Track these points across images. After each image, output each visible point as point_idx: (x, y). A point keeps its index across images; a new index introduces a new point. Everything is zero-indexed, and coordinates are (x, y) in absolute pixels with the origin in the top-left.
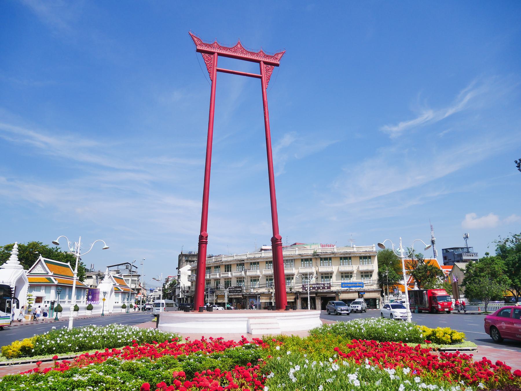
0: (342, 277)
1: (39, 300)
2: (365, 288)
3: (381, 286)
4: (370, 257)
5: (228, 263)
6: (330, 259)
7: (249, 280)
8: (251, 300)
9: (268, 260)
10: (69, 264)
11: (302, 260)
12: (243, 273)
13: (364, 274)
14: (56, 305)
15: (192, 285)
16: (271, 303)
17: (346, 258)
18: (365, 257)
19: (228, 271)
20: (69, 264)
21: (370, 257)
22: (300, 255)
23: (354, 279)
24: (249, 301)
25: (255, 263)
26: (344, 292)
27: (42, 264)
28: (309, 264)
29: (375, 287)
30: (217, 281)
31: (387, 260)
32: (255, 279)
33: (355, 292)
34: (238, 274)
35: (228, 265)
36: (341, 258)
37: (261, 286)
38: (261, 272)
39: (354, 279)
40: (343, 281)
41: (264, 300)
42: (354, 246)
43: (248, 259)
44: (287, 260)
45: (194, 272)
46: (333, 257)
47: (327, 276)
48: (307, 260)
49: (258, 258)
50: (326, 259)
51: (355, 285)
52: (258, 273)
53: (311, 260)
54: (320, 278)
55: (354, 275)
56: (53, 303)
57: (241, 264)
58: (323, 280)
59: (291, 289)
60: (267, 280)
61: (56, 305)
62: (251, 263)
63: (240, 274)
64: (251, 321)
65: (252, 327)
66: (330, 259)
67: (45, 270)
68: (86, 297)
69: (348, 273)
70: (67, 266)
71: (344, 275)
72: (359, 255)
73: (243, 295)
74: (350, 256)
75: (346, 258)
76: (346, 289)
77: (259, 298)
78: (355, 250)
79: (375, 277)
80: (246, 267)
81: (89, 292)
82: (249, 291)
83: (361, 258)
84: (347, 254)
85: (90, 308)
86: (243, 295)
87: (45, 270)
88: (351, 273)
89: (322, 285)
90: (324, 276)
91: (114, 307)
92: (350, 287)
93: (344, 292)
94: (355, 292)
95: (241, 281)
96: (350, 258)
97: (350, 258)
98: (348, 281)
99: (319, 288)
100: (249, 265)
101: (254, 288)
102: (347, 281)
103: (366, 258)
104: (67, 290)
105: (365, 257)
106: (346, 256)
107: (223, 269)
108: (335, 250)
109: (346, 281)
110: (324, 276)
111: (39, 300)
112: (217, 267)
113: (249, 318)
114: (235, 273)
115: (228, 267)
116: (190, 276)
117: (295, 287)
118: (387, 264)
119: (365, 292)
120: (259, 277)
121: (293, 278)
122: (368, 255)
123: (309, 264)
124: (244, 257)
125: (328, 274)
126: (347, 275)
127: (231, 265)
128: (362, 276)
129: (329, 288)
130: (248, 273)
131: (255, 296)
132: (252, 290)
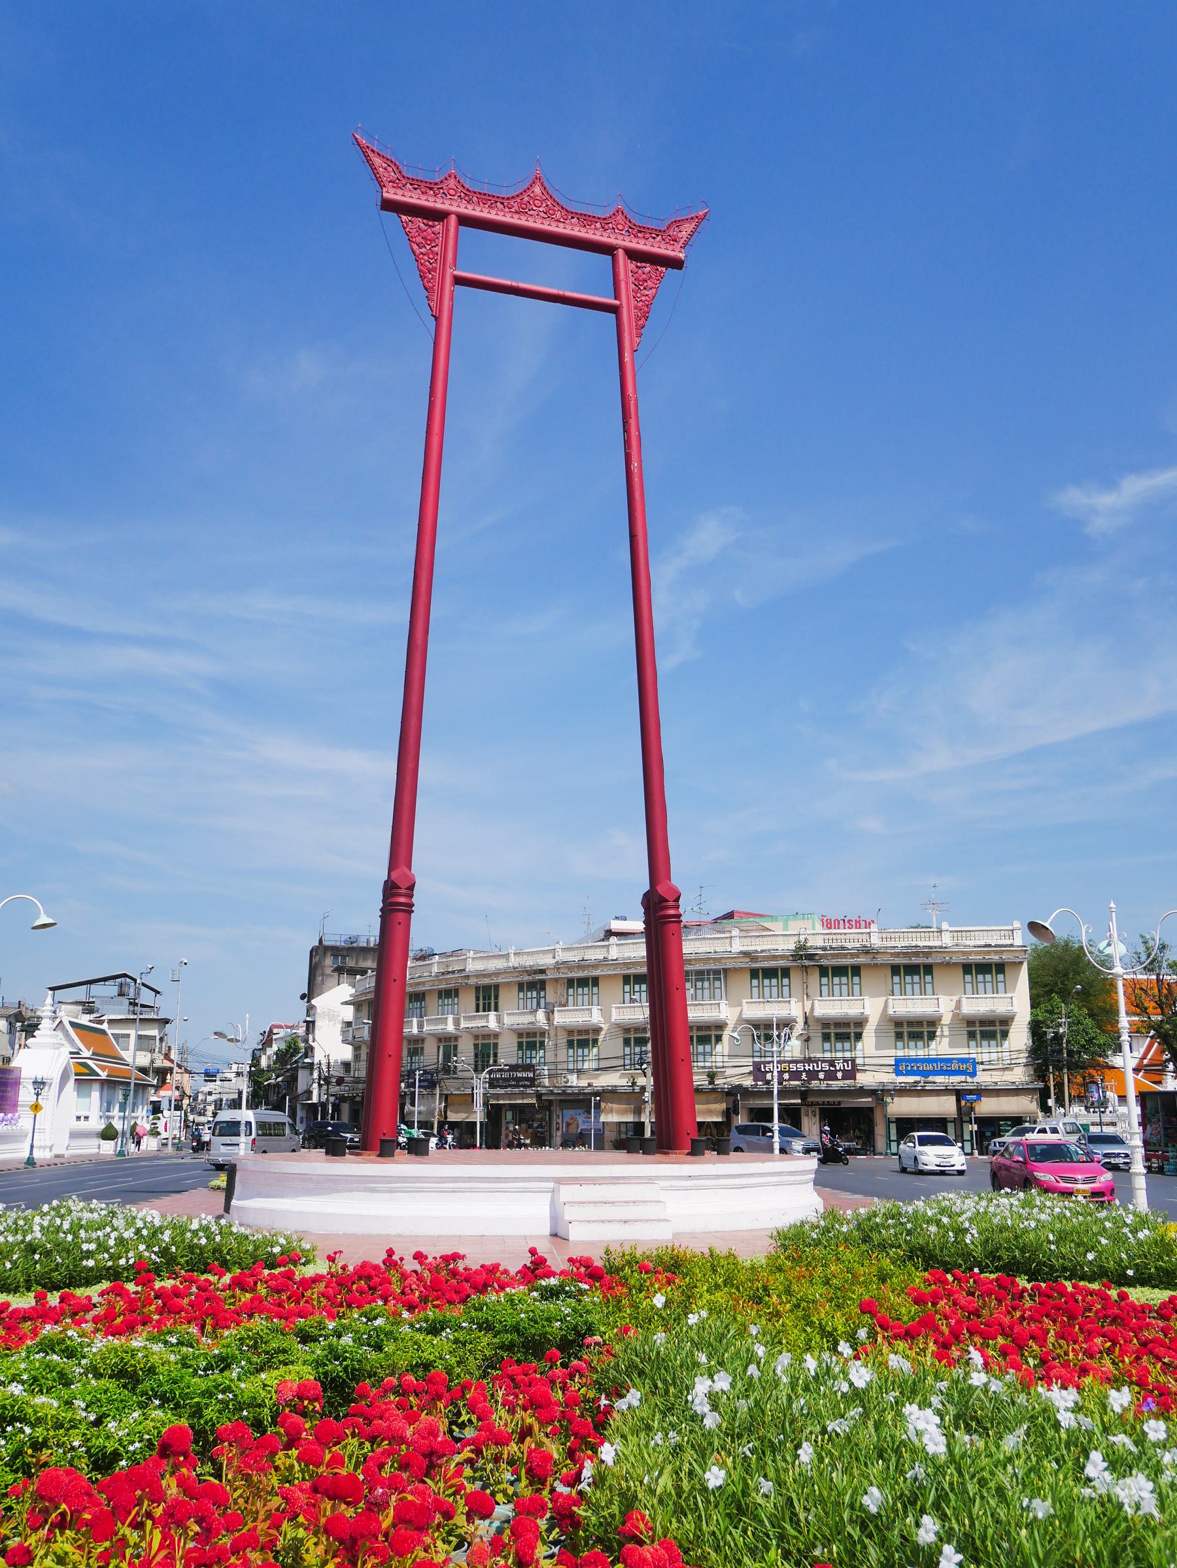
0: (899, 1036)
2: (983, 1078)
3: (1040, 1073)
4: (1000, 968)
5: (487, 981)
6: (856, 970)
7: (563, 1041)
8: (568, 1113)
9: (632, 971)
11: (754, 973)
12: (541, 1015)
13: (978, 1029)
15: (357, 1057)
16: (639, 1126)
17: (914, 968)
18: (984, 968)
19: (487, 1008)
21: (1000, 968)
22: (746, 954)
23: (941, 1047)
24: (563, 1119)
25: (583, 982)
26: (903, 1091)
28: (780, 987)
29: (1019, 1075)
30: (449, 1043)
31: (1064, 977)
32: (583, 1039)
33: (946, 1091)
34: (522, 1020)
35: (487, 988)
36: (895, 970)
37: (603, 1064)
38: (606, 1014)
39: (941, 1047)
40: (900, 1053)
41: (614, 1116)
42: (945, 926)
43: (558, 967)
45: (365, 1010)
46: (868, 966)
47: (846, 1031)
48: (770, 973)
49: (597, 965)
50: (840, 971)
51: (945, 1066)
53: (786, 972)
54: (817, 1040)
55: (943, 1031)
57: (534, 983)
58: (827, 1046)
59: (712, 1076)
60: (627, 1042)
62: (570, 983)
63: (530, 1018)
64: (567, 1193)
65: (569, 1214)
66: (856, 970)
69: (919, 1023)
71: (905, 1030)
72: (962, 959)
73: (539, 1096)
74: (930, 961)
75: (914, 968)
76: (911, 1079)
77: (598, 1106)
78: (947, 940)
79: (1020, 1038)
80: (550, 995)
82: (561, 1082)
83: (967, 968)
84: (917, 954)
86: (539, 1096)
89: (826, 1067)
90: (832, 1031)
91: (74, 1135)
92: (925, 1074)
93: (903, 1091)
94: (946, 1091)
95: (532, 1046)
96: (928, 969)
97: (928, 969)
99: (813, 1075)
100: (561, 989)
101: (579, 1072)
102: (915, 1051)
103: (986, 969)
105: (984, 968)
106: (915, 960)
107: (468, 1000)
108: (876, 941)
110: (832, 1031)
112: (449, 994)
113: (560, 1181)
114: (511, 1017)
115: (487, 996)
116: (349, 1024)
117: (729, 1072)
118: (1065, 995)
119: (981, 1092)
120: (597, 1030)
121: (719, 1039)
122: (996, 958)
123: (780, 987)
124: (547, 961)
125: (847, 1025)
126: (918, 1030)
127: (497, 987)
128: (971, 1035)
129: (850, 1074)
130: (559, 1018)
131: (583, 1101)
132: (573, 1080)
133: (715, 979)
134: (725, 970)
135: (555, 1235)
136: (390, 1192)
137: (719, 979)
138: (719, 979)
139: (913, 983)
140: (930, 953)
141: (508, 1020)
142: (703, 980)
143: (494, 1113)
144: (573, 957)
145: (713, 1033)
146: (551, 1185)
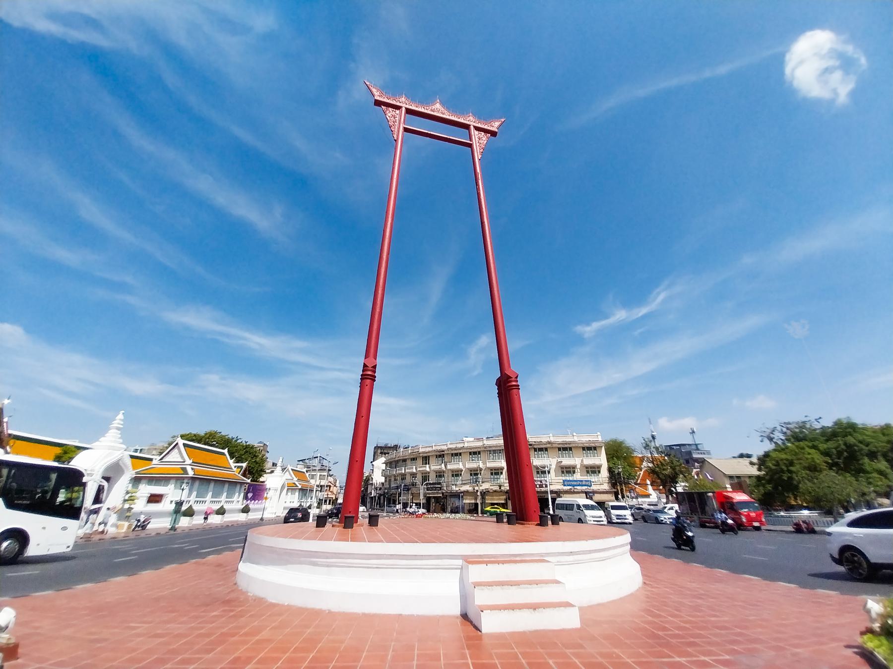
0: (563, 472)
1: (155, 499)
2: (594, 488)
3: (614, 485)
4: (595, 448)
6: (546, 449)
8: (453, 499)
10: (226, 451)
12: (443, 465)
14: (184, 508)
16: (476, 504)
17: (565, 449)
18: (589, 449)
20: (226, 451)
21: (595, 448)
23: (578, 476)
24: (452, 503)
25: (456, 455)
26: (567, 492)
27: (179, 449)
29: (606, 487)
30: (414, 475)
31: (617, 452)
32: (457, 474)
33: (582, 492)
35: (426, 457)
36: (559, 449)
38: (464, 465)
39: (578, 476)
41: (468, 501)
50: (541, 450)
51: (581, 483)
52: (461, 466)
55: (578, 470)
56: (179, 504)
57: (441, 455)
59: (500, 486)
60: (471, 475)
61: (184, 508)
63: (439, 467)
64: (477, 573)
65: (481, 597)
66: (546, 449)
67: (182, 457)
68: (242, 495)
69: (569, 468)
70: (223, 454)
75: (565, 449)
76: (569, 487)
78: (576, 439)
79: (604, 473)
80: (446, 459)
81: (249, 489)
83: (584, 449)
85: (246, 510)
87: (182, 457)
88: (574, 467)
92: (574, 486)
93: (567, 492)
94: (582, 492)
95: (440, 476)
96: (571, 449)
97: (571, 449)
98: (571, 478)
103: (590, 449)
104: (238, 487)
105: (589, 449)
107: (420, 461)
108: (552, 439)
109: (568, 478)
111: (155, 499)
112: (413, 459)
113: (470, 560)
114: (433, 466)
115: (426, 459)
118: (618, 458)
119: (594, 492)
124: (445, 448)
126: (569, 470)
128: (588, 472)
130: (449, 467)
131: (457, 495)
135: (465, 616)
136: (328, 566)
141: (433, 468)
143: (428, 499)
144: (453, 446)
146: (460, 562)
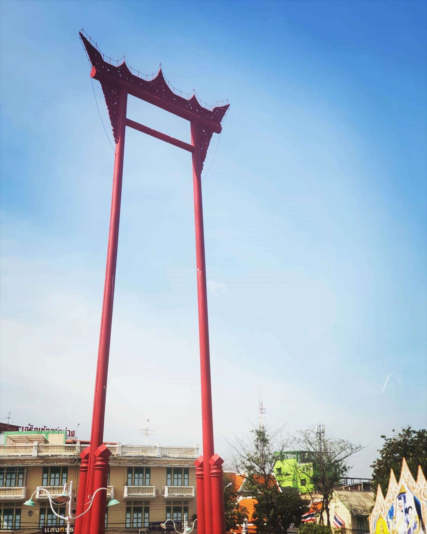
36: (130, 470)
44: (9, 469)
48: (55, 470)
53: (65, 470)
133: (19, 473)
134: (27, 467)
137: (23, 473)
138: (23, 473)
139: (139, 478)
140: (149, 461)
142: (11, 474)
145: (15, 507)
